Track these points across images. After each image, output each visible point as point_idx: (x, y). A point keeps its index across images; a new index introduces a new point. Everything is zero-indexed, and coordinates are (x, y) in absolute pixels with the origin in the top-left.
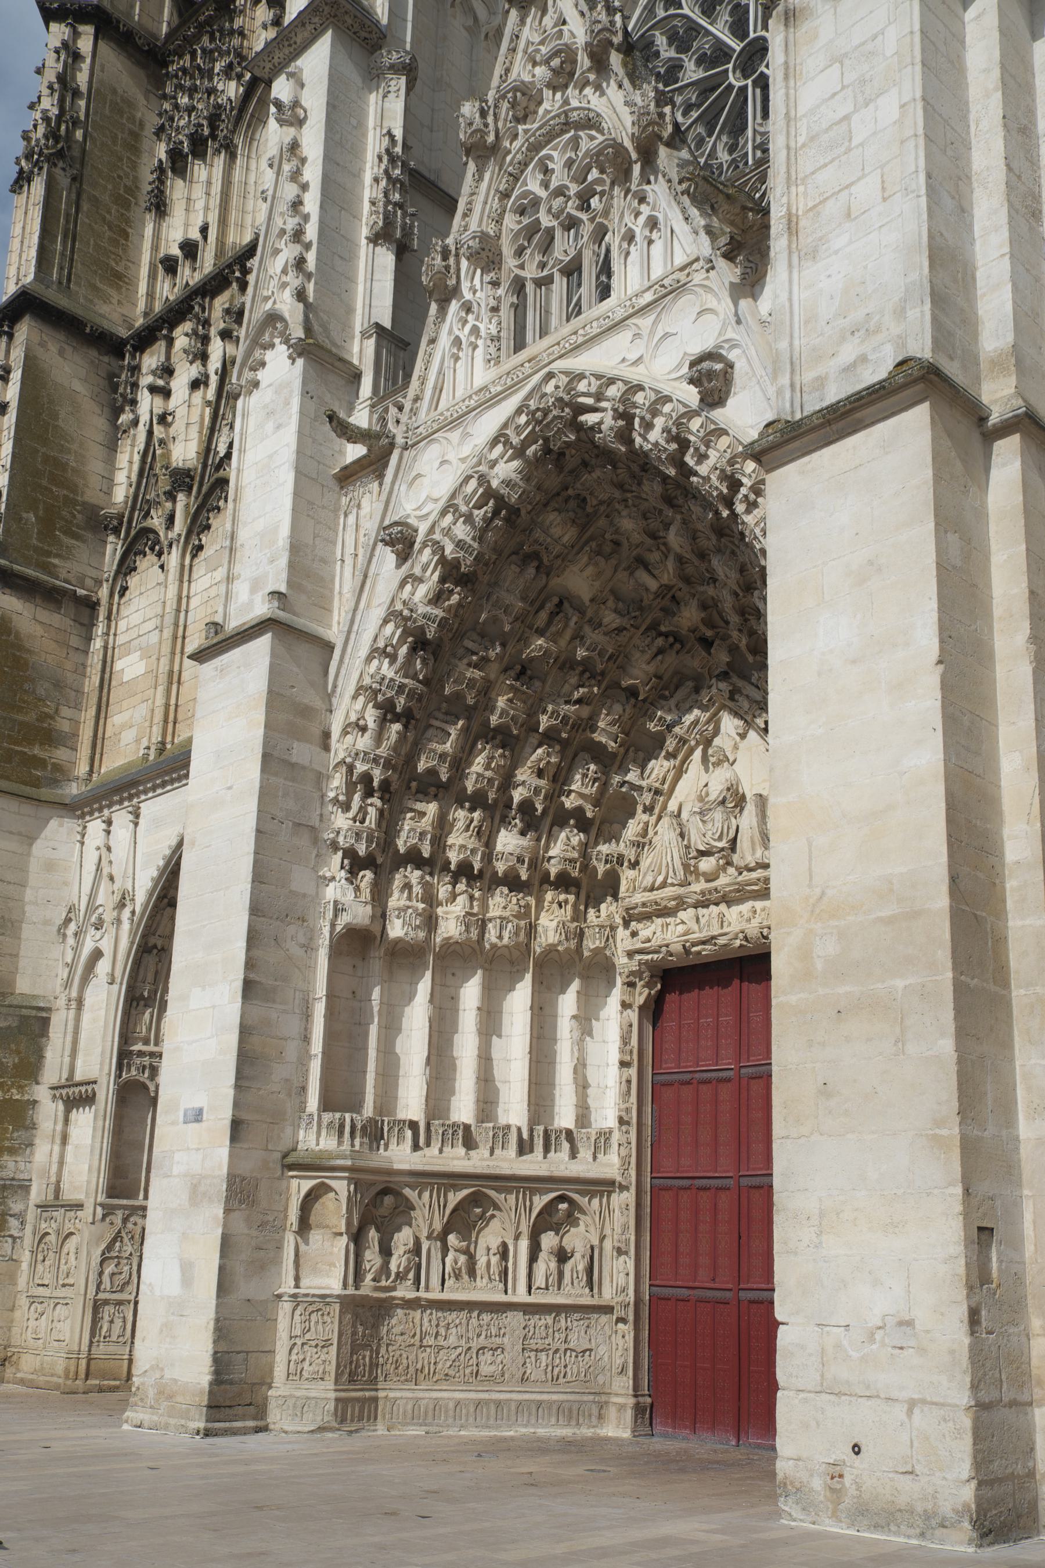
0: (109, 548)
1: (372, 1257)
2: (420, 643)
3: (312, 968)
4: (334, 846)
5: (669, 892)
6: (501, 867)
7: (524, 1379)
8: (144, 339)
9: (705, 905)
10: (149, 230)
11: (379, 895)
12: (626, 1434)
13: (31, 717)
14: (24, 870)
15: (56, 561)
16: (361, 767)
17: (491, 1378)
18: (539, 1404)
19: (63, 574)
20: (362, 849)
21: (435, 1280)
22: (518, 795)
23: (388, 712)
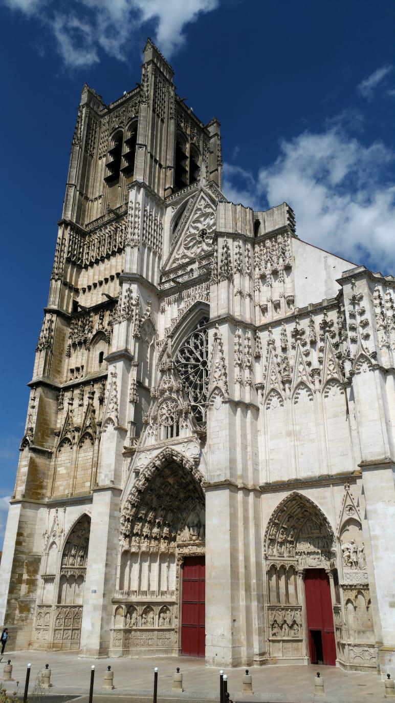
0: (56, 440)
1: (128, 620)
2: (139, 491)
3: (117, 559)
4: (121, 533)
5: (186, 542)
6: (154, 535)
7: (157, 645)
8: (67, 389)
9: (193, 546)
10: (67, 361)
11: (130, 542)
12: (177, 656)
13: (38, 483)
14: (35, 521)
15: (44, 444)
16: (127, 517)
17: (151, 645)
18: (160, 650)
19: (46, 447)
20: (127, 534)
21: (140, 625)
22: (157, 521)
23: (133, 506)
